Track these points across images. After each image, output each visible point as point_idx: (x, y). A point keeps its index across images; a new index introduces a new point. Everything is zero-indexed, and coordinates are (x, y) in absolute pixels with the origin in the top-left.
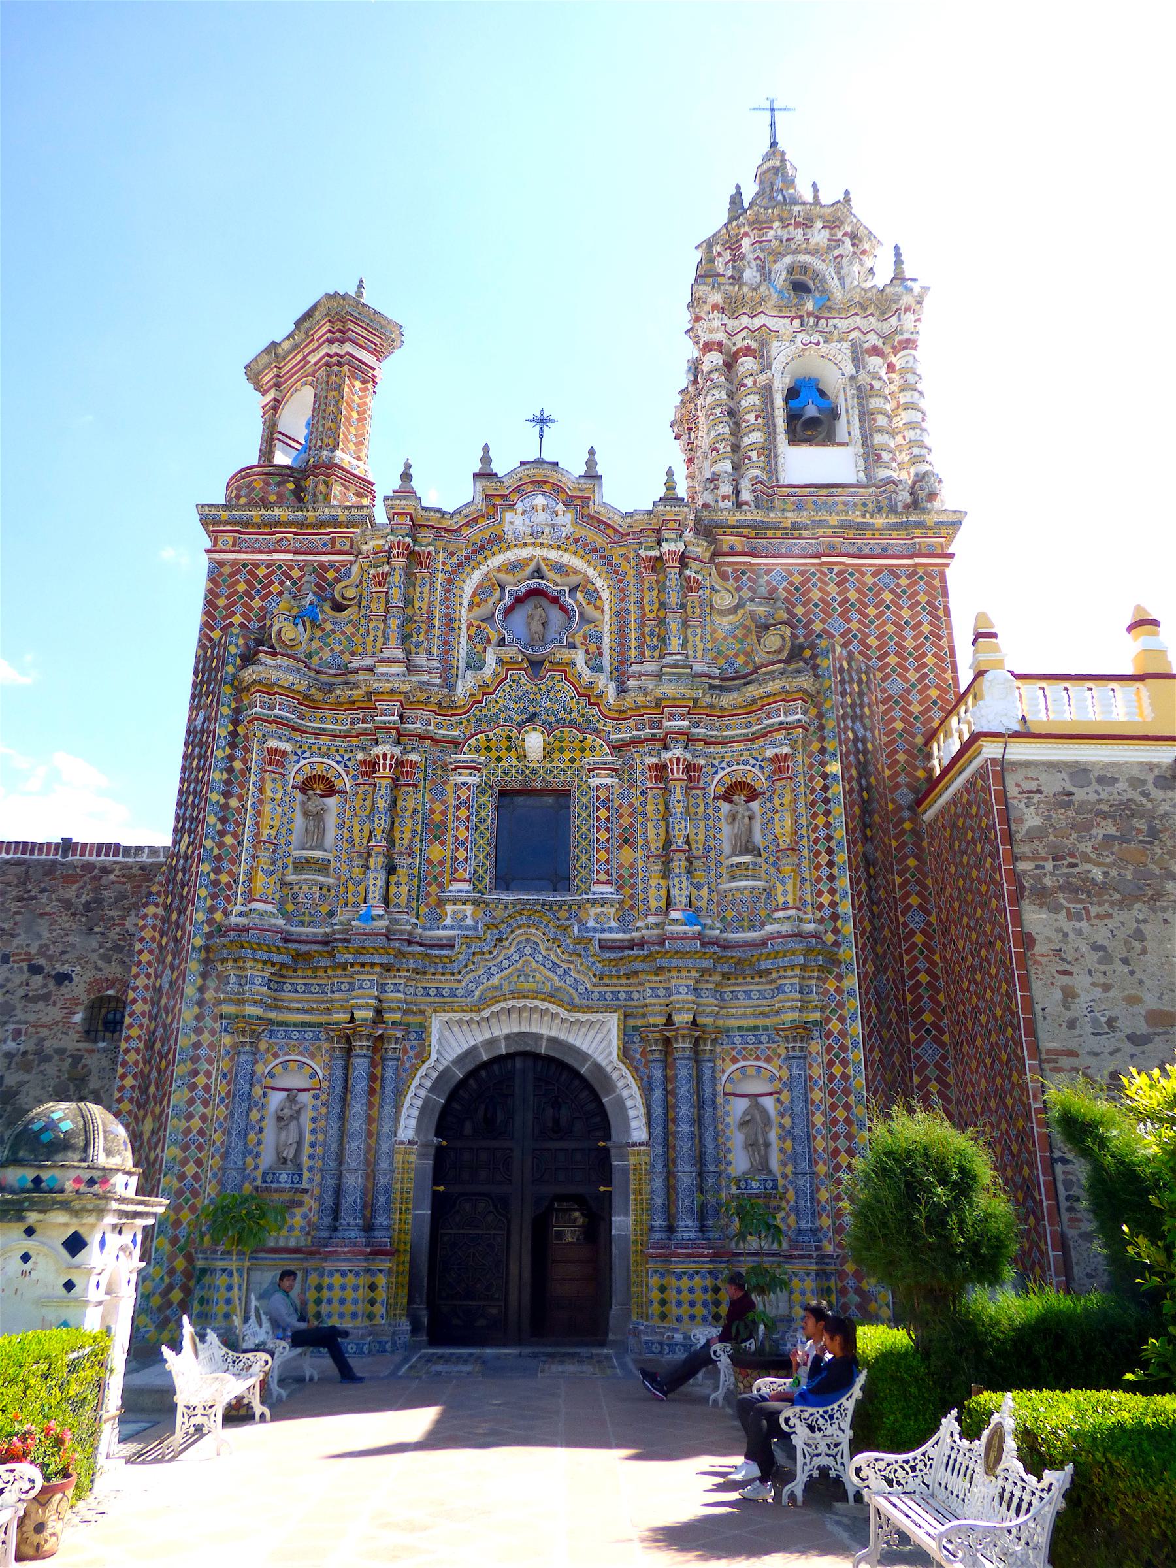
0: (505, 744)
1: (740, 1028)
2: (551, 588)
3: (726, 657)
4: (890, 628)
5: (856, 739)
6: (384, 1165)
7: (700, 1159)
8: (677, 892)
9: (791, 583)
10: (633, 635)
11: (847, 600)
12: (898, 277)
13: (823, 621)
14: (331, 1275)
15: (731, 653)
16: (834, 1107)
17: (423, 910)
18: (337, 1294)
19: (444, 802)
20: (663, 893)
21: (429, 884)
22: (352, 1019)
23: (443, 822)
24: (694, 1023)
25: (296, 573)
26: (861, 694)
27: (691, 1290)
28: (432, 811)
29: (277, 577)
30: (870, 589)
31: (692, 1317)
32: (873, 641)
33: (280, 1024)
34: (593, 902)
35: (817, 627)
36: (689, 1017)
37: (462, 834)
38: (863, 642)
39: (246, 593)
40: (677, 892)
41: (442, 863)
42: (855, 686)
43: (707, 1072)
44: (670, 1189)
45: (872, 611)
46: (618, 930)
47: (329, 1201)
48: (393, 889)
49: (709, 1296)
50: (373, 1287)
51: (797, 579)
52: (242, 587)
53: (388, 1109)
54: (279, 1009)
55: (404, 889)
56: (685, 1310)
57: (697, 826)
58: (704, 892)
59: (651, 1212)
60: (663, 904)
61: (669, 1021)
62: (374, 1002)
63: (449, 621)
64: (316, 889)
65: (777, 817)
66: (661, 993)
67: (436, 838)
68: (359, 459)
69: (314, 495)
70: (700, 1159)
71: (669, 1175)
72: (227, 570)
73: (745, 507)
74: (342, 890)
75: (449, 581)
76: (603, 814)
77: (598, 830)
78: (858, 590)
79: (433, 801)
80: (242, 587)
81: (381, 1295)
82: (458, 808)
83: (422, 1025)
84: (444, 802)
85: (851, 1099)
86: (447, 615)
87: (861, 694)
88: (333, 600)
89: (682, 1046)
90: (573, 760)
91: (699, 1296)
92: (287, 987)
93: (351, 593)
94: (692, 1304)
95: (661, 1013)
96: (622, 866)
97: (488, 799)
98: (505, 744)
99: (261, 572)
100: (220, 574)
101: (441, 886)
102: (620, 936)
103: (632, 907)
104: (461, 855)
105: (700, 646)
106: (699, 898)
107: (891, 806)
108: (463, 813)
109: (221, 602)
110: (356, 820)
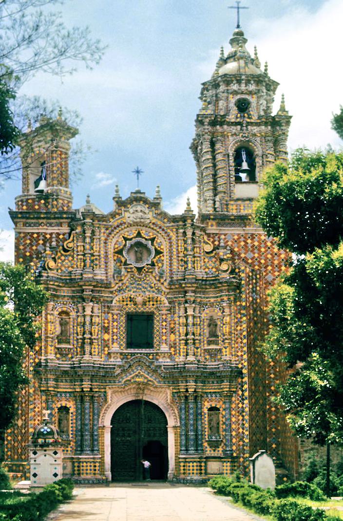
0: (129, 299)
1: (210, 392)
2: (143, 241)
3: (209, 268)
4: (269, 256)
5: (253, 299)
6: (96, 433)
7: (196, 430)
8: (190, 351)
9: (234, 239)
10: (175, 260)
11: (254, 245)
12: (282, 109)
13: (245, 254)
14: (83, 463)
15: (210, 267)
16: (238, 416)
17: (103, 355)
18: (85, 468)
19: (108, 320)
20: (185, 350)
21: (104, 347)
22: (83, 391)
23: (108, 327)
24: (195, 391)
25: (48, 236)
26: (256, 283)
27: (193, 466)
28: (104, 323)
29: (41, 237)
30: (263, 241)
31: (193, 473)
32: (263, 261)
33: (58, 392)
34: (161, 353)
35: (243, 255)
36: (193, 390)
37: (115, 330)
38: (259, 262)
39: (30, 244)
40: (190, 351)
41: (108, 340)
42: (254, 281)
43: (199, 406)
44: (187, 439)
45: (263, 250)
46: (169, 362)
47: (79, 443)
48: (93, 350)
49: (198, 468)
50: (95, 466)
51: (236, 237)
52: (28, 242)
53: (96, 417)
54: (58, 388)
55: (97, 350)
56: (191, 472)
57: (197, 328)
58: (199, 350)
59: (181, 446)
60: (185, 354)
61: (187, 391)
62: (90, 386)
63: (106, 256)
64: (67, 350)
65: (224, 326)
66: (184, 382)
67: (106, 332)
68: (67, 187)
69: (52, 205)
70: (196, 430)
71: (186, 435)
72: (22, 235)
73: (217, 210)
74: (75, 350)
75: (106, 240)
76: (164, 324)
77: (163, 329)
78: (258, 242)
79: (104, 319)
80: (28, 242)
81: (97, 468)
82: (113, 322)
83: (105, 392)
84: (108, 320)
85: (244, 414)
86: (106, 253)
87: (256, 283)
88: (63, 246)
89: (191, 400)
90: (153, 305)
91: (195, 468)
92: (60, 381)
93: (71, 245)
94: (193, 470)
95: (184, 389)
96: (171, 341)
97: (123, 319)
98: (129, 299)
99: (35, 235)
100: (20, 237)
101: (109, 347)
102: (170, 364)
103: (175, 354)
104: (115, 337)
105: (199, 265)
106: (197, 352)
107: (265, 320)
108: (115, 324)
109: (21, 247)
110: (79, 327)
